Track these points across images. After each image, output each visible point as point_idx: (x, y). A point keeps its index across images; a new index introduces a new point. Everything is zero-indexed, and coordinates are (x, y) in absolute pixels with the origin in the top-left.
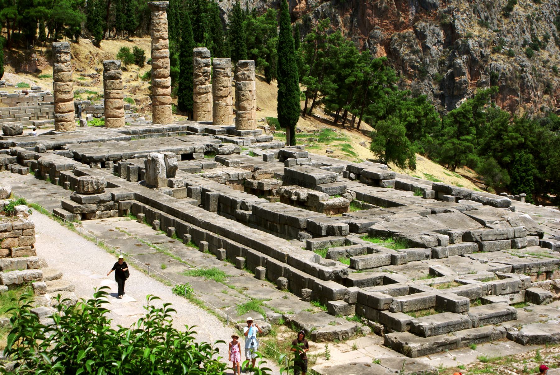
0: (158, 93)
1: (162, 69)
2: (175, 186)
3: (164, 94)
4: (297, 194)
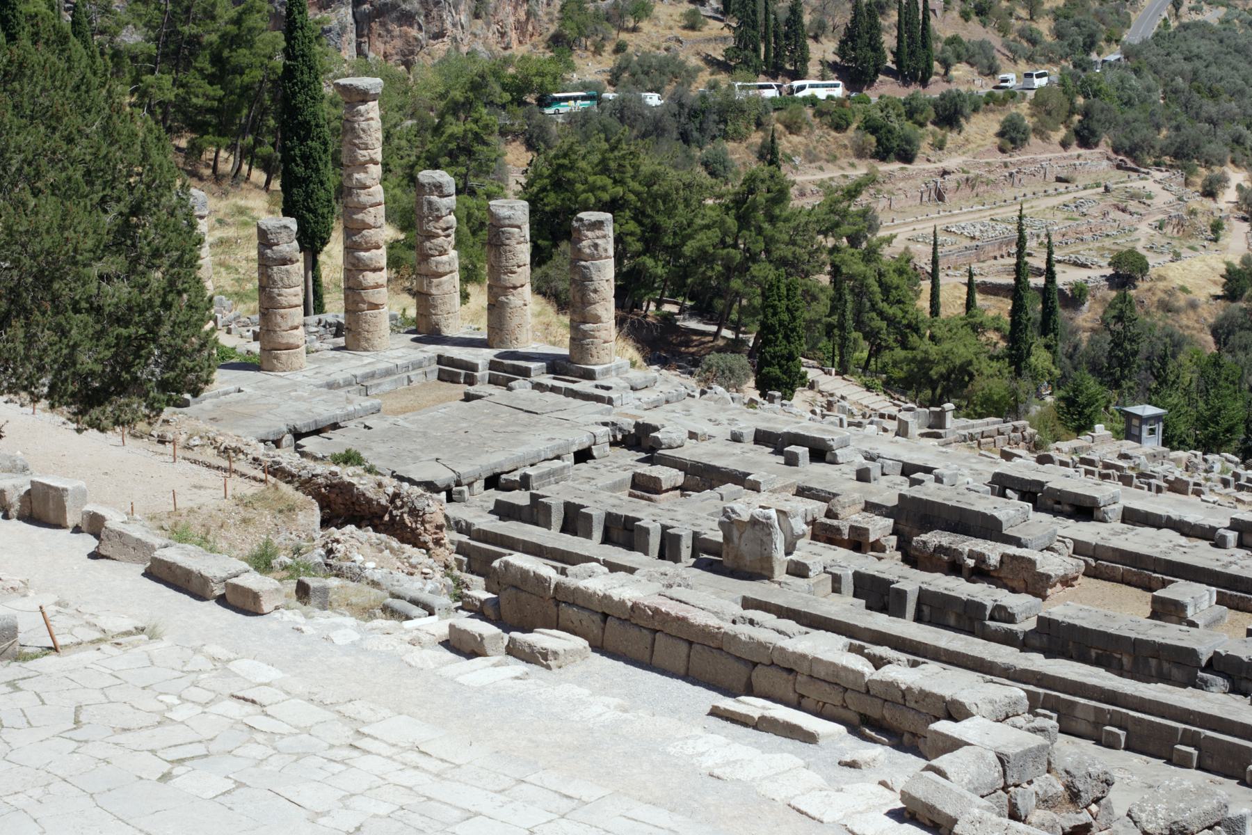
0: (365, 283)
1: (372, 231)
2: (811, 574)
3: (377, 286)
4: (981, 558)
